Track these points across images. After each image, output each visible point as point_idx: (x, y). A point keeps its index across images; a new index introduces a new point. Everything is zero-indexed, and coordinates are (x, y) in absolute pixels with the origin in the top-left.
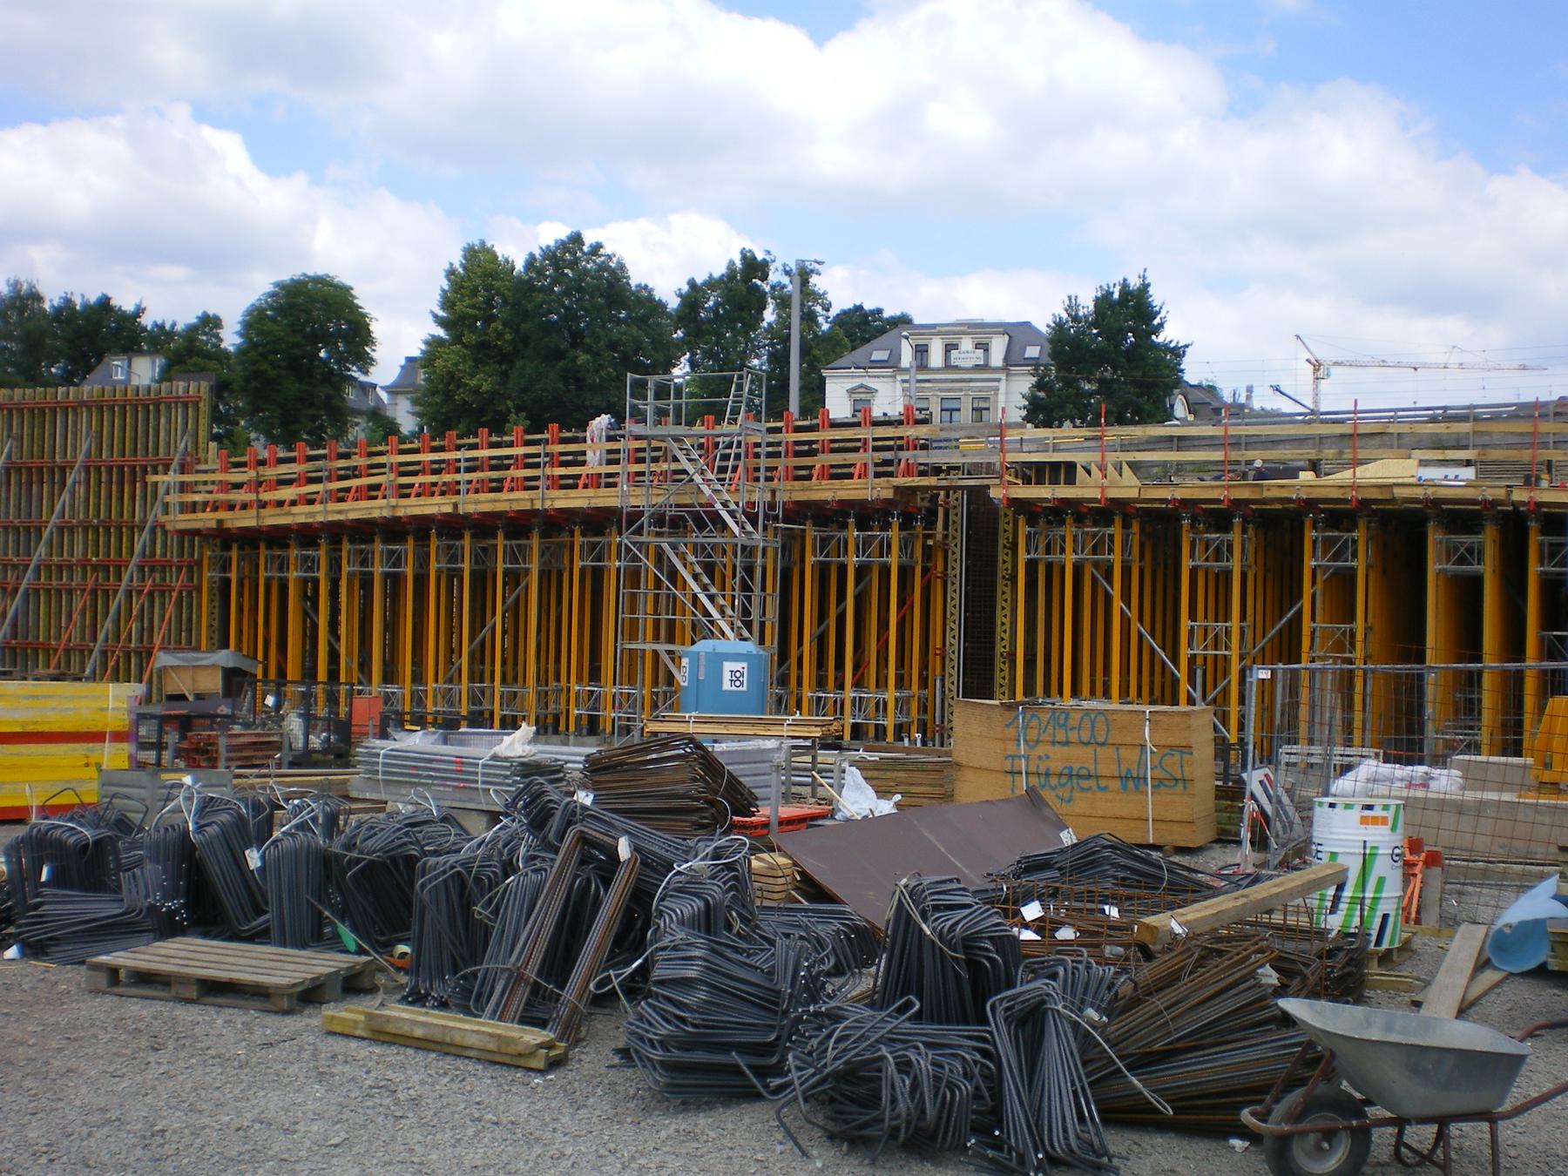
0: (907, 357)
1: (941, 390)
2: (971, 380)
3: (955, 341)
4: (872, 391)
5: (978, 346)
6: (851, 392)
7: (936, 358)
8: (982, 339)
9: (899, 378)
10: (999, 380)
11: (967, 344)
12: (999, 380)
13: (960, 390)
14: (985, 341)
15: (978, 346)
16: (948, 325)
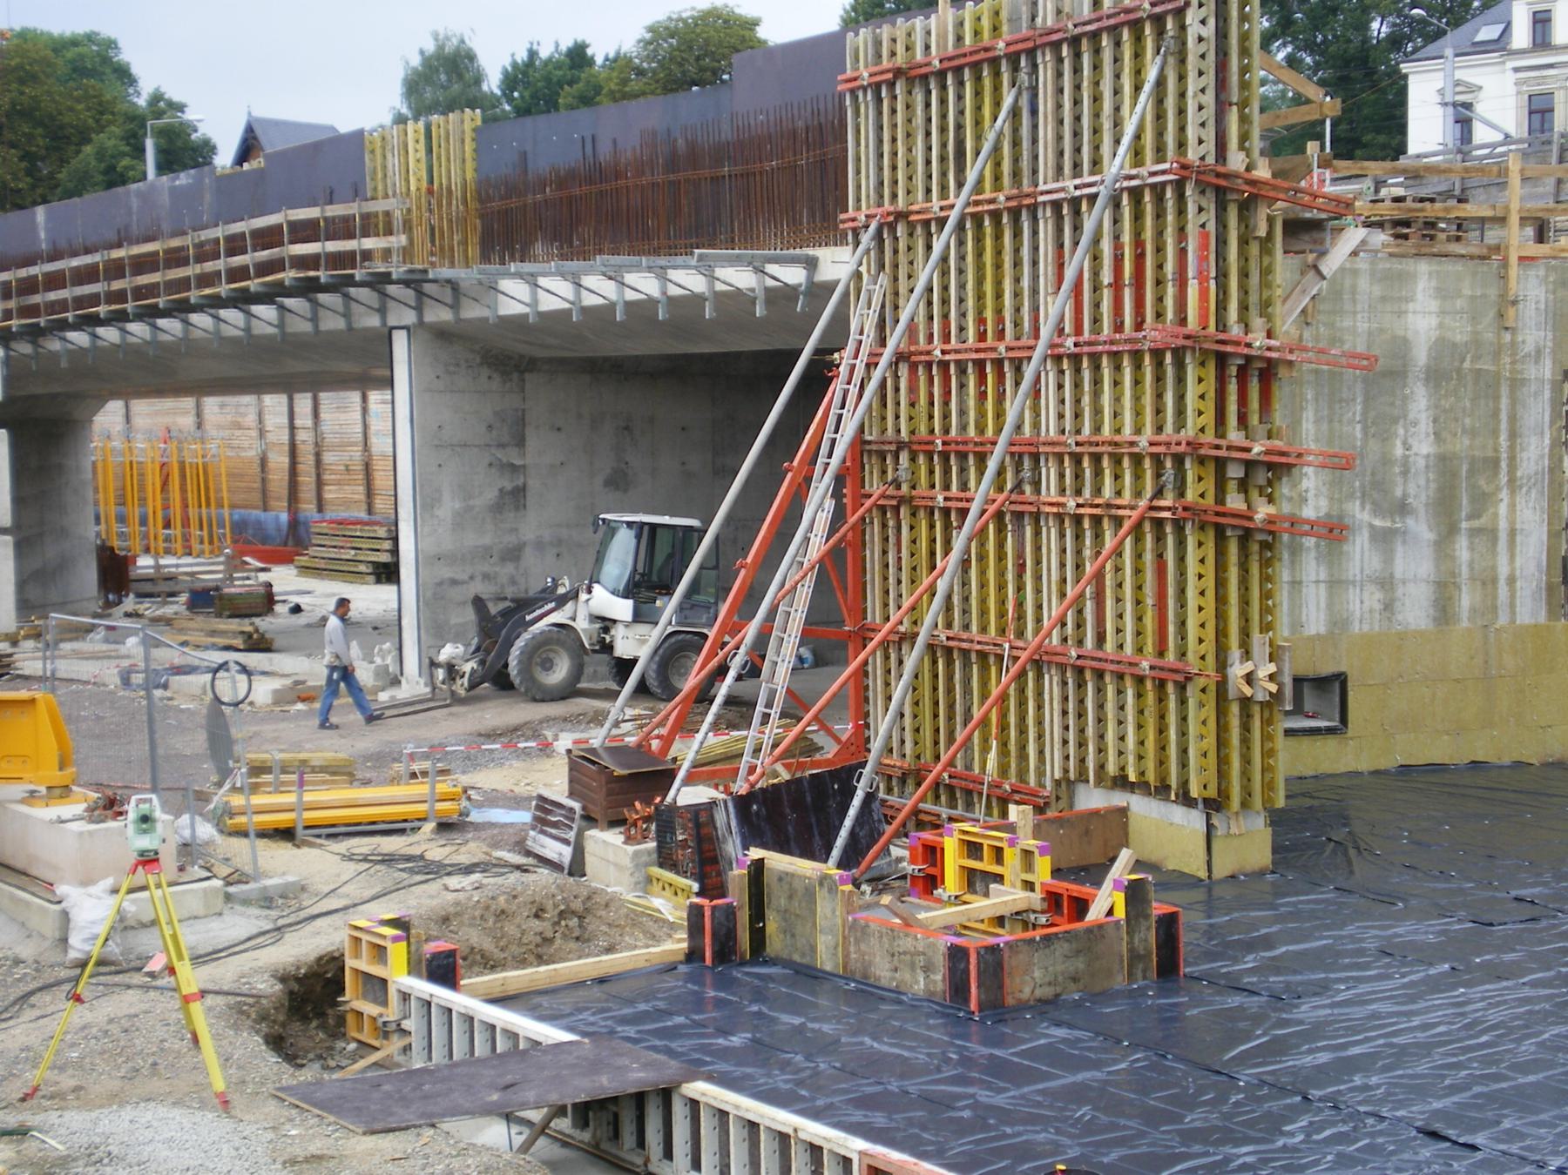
0: (1521, 36)
9: (1510, 64)
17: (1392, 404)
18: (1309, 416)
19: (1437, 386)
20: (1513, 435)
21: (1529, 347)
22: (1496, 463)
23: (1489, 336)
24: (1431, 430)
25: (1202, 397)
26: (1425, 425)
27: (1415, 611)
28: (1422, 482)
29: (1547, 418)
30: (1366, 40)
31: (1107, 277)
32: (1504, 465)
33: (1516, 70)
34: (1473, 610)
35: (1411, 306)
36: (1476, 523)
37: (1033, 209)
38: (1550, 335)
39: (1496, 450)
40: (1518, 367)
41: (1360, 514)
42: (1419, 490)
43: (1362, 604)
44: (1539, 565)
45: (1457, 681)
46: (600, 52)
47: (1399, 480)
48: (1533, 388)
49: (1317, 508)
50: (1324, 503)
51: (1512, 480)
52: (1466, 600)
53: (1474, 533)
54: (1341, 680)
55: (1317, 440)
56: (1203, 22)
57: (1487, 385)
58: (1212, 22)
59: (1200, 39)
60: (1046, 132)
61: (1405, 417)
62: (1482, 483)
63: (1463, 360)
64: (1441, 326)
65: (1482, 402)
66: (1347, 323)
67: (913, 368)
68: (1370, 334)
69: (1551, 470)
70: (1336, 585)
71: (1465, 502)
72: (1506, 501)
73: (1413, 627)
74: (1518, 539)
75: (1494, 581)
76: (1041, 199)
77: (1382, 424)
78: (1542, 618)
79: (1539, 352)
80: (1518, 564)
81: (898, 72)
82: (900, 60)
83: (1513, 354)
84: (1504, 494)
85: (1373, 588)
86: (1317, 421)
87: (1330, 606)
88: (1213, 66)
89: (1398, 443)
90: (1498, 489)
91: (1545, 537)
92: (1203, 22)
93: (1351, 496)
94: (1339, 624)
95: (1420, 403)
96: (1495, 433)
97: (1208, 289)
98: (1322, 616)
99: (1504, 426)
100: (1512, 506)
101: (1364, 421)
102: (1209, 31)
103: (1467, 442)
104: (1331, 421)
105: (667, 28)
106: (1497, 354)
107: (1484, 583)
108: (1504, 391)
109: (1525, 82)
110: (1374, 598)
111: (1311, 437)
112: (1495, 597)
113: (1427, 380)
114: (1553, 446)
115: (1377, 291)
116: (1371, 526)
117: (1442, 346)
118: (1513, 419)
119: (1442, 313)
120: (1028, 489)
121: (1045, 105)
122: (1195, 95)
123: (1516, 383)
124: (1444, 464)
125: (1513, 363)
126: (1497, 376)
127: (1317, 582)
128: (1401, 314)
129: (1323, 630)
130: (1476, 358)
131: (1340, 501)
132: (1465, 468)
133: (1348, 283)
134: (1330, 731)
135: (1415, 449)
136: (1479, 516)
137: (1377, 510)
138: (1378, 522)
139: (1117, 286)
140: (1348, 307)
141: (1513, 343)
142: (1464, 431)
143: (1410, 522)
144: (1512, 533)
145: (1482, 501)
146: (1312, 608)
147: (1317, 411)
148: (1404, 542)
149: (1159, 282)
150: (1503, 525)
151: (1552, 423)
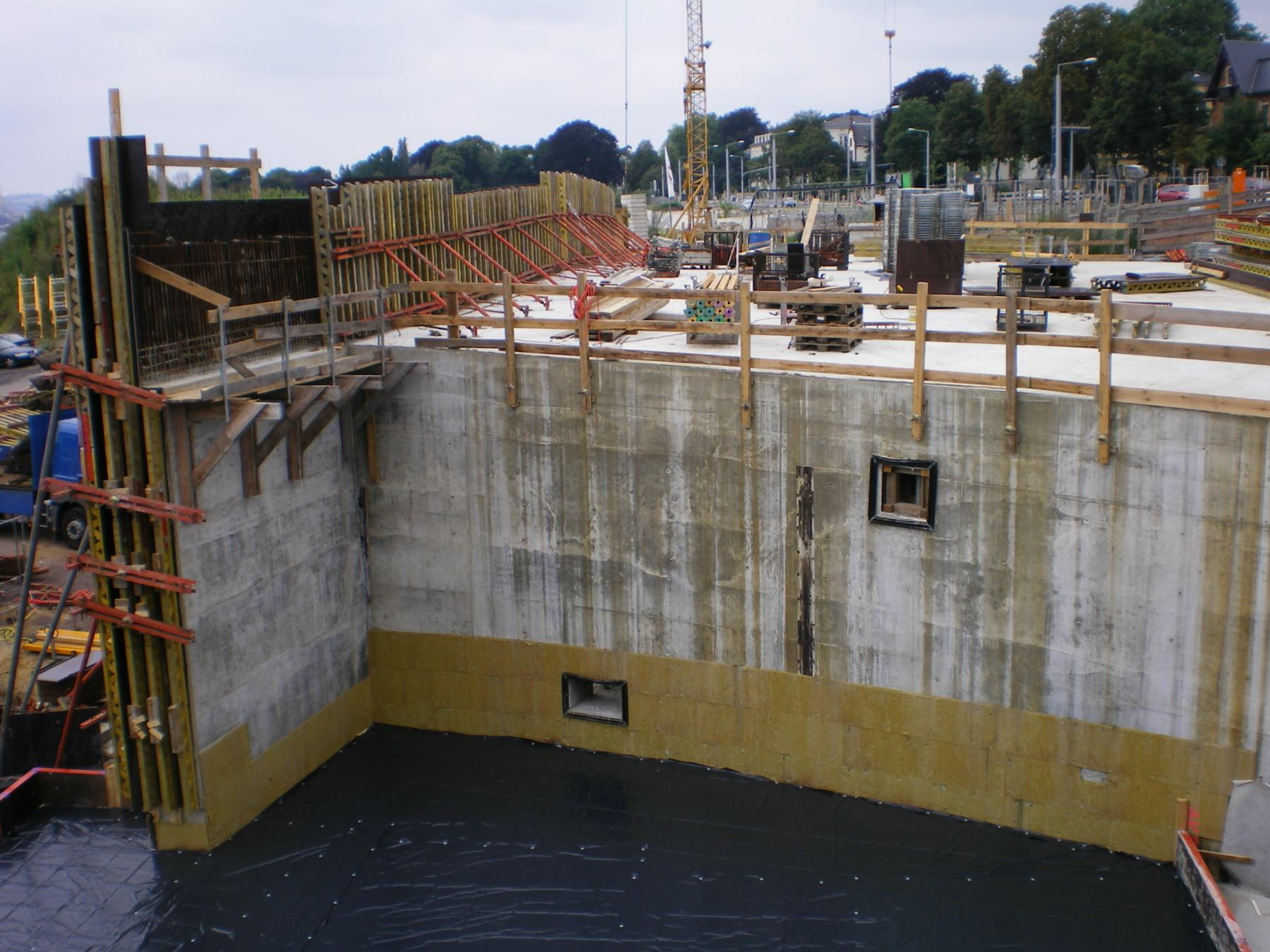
17: (658, 481)
18: (593, 483)
19: (693, 470)
20: (756, 516)
21: (768, 445)
22: (742, 537)
23: (734, 433)
24: (689, 505)
26: (684, 500)
27: (680, 645)
28: (683, 545)
29: (784, 506)
32: (748, 539)
34: (726, 651)
35: (669, 404)
36: (727, 583)
38: (785, 436)
39: (742, 527)
40: (759, 460)
41: (636, 563)
42: (681, 550)
43: (639, 633)
44: (779, 624)
45: (713, 704)
46: (1014, 73)
47: (665, 540)
48: (772, 479)
49: (602, 555)
50: (607, 551)
51: (756, 553)
52: (720, 643)
53: (725, 590)
54: (623, 686)
55: (600, 503)
57: (735, 473)
61: (668, 491)
62: (731, 551)
63: (713, 451)
64: (694, 422)
65: (730, 486)
66: (619, 414)
68: (638, 423)
69: (788, 548)
70: (618, 614)
72: (750, 569)
73: (678, 656)
74: (762, 600)
75: (743, 631)
77: (652, 495)
78: (782, 667)
79: (776, 450)
80: (762, 620)
83: (755, 450)
84: (749, 563)
85: (647, 621)
86: (600, 488)
87: (614, 630)
89: (663, 512)
90: (744, 558)
91: (784, 602)
93: (628, 549)
94: (622, 644)
95: (679, 482)
96: (741, 512)
98: (609, 636)
99: (748, 507)
100: (756, 574)
101: (636, 492)
103: (718, 518)
104: (610, 489)
106: (741, 448)
107: (734, 632)
108: (748, 479)
110: (648, 630)
111: (596, 500)
112: (743, 645)
113: (685, 464)
114: (789, 530)
115: (641, 391)
116: (644, 574)
117: (695, 438)
118: (755, 503)
119: (694, 411)
123: (757, 474)
124: (700, 532)
125: (755, 456)
126: (741, 466)
127: (604, 610)
128: (662, 410)
129: (609, 647)
130: (723, 450)
131: (620, 552)
132: (717, 538)
133: (618, 382)
134: (614, 722)
135: (676, 519)
136: (729, 578)
137: (649, 562)
138: (649, 572)
140: (619, 401)
141: (754, 440)
142: (716, 508)
143: (674, 575)
144: (757, 596)
145: (732, 567)
146: (601, 629)
147: (598, 482)
148: (670, 589)
150: (749, 587)
151: (788, 510)
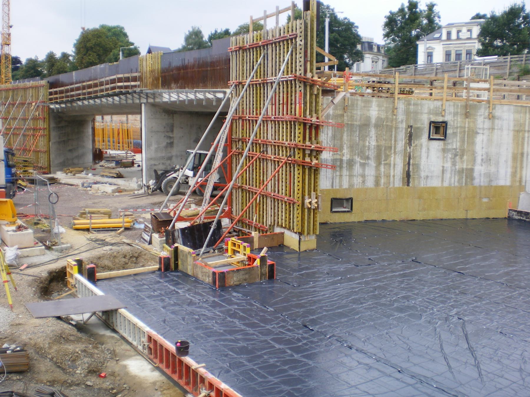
0: (444, 37)
1: (455, 47)
2: (465, 43)
3: (460, 29)
4: (433, 49)
5: (468, 31)
6: (427, 49)
7: (454, 36)
8: (469, 28)
9: (442, 43)
10: (475, 43)
11: (464, 30)
12: (475, 43)
13: (462, 47)
14: (470, 29)
15: (468, 31)
16: (461, 23)
17: (366, 132)
18: (345, 135)
19: (377, 128)
20: (395, 141)
21: (400, 120)
22: (391, 147)
23: (390, 117)
24: (375, 139)
25: (300, 133)
26: (374, 138)
27: (370, 183)
28: (373, 152)
29: (404, 137)
30: (411, 35)
31: (281, 102)
32: (393, 148)
33: (443, 45)
34: (384, 183)
35: (371, 109)
36: (386, 162)
37: (267, 83)
38: (405, 117)
39: (391, 145)
40: (397, 124)
41: (357, 159)
42: (372, 154)
43: (357, 181)
44: (401, 172)
45: (380, 200)
47: (367, 151)
48: (401, 130)
49: (347, 157)
50: (348, 156)
51: (395, 152)
52: (382, 181)
53: (385, 164)
54: (351, 199)
55: (347, 141)
56: (301, 41)
57: (389, 129)
58: (303, 41)
59: (300, 45)
60: (270, 65)
61: (369, 135)
62: (387, 152)
63: (384, 122)
64: (378, 114)
65: (388, 133)
66: (355, 112)
67: (243, 120)
68: (361, 115)
69: (404, 150)
70: (351, 176)
71: (383, 157)
72: (393, 157)
73: (369, 187)
74: (396, 166)
75: (390, 176)
76: (268, 81)
77: (363, 137)
78: (401, 185)
79: (402, 121)
80: (396, 172)
81: (240, 48)
82: (241, 45)
83: (396, 121)
84: (393, 155)
85: (360, 177)
86: (347, 136)
87: (349, 181)
88: (303, 51)
89: (367, 142)
90: (391, 154)
91: (402, 166)
92: (301, 41)
93: (355, 154)
94: (351, 185)
95: (373, 132)
96: (391, 140)
97: (301, 107)
98: (347, 184)
99: (393, 138)
100: (395, 158)
101: (359, 136)
102: (302, 43)
103: (384, 142)
104: (351, 136)
105: (243, 27)
106: (392, 121)
107: (387, 177)
108: (394, 130)
109: (445, 47)
110: (360, 180)
111: (346, 140)
112: (390, 180)
113: (375, 127)
114: (405, 144)
115: (363, 105)
116: (360, 162)
117: (378, 119)
118: (395, 137)
119: (379, 110)
120: (265, 153)
121: (270, 58)
122: (299, 59)
123: (397, 128)
124: (378, 148)
125: (396, 123)
126: (392, 126)
127: (346, 175)
128: (369, 110)
129: (347, 187)
130: (387, 122)
131: (352, 156)
132: (383, 149)
133: (355, 102)
134: (348, 212)
135: (371, 144)
136: (386, 161)
137: (362, 158)
138: (361, 161)
139: (283, 104)
140: (355, 108)
141: (396, 119)
142: (383, 139)
143: (370, 161)
144: (394, 165)
145: (387, 157)
146: (345, 181)
147: (347, 134)
148: (368, 166)
149: (291, 104)
150: (392, 163)
151: (405, 138)
